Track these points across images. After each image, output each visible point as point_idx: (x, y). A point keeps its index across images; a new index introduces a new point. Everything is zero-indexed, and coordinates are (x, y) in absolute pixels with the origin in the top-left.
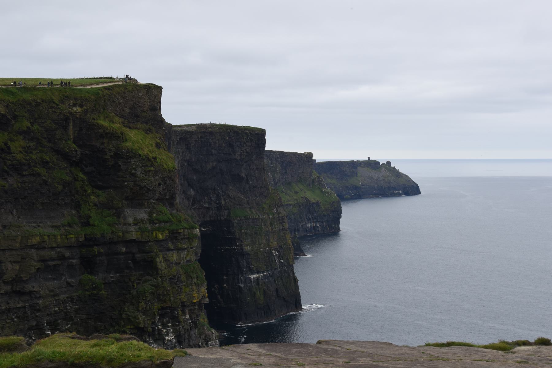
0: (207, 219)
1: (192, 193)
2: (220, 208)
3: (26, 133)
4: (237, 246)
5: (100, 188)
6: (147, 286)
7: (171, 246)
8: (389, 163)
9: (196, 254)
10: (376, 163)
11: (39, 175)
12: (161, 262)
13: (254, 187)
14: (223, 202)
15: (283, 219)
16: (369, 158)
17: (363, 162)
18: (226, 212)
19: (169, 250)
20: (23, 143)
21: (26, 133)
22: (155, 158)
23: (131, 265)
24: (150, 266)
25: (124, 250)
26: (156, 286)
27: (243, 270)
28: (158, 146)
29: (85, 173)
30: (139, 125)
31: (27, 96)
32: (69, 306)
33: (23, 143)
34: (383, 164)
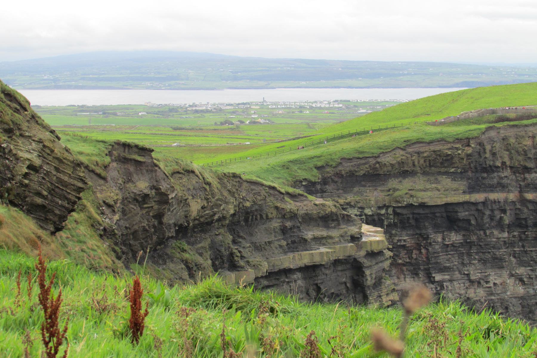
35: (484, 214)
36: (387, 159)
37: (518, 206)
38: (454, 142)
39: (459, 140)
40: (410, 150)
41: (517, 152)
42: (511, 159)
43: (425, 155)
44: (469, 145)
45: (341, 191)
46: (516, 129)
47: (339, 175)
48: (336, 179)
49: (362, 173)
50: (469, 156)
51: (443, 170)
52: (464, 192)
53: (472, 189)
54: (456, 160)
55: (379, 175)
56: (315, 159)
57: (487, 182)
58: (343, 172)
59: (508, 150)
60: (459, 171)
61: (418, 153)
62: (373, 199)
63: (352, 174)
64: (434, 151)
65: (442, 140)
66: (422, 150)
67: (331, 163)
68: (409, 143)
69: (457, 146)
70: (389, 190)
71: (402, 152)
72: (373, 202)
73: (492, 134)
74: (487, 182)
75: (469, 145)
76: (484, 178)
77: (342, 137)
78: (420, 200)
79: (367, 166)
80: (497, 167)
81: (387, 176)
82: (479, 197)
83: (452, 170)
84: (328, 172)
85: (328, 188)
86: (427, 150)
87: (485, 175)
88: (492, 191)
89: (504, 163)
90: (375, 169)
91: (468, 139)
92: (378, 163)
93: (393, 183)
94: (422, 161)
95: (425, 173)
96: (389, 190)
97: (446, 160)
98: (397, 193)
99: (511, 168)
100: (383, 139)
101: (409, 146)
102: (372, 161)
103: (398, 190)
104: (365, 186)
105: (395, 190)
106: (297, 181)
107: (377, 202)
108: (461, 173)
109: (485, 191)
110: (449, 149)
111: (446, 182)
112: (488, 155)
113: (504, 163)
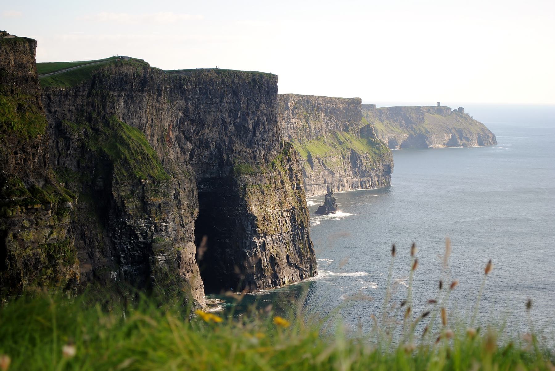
0: (208, 176)
1: (189, 146)
2: (221, 164)
4: (241, 206)
8: (461, 109)
9: (192, 215)
10: (447, 109)
12: (9, 241)
13: (263, 140)
14: (225, 157)
15: (296, 176)
16: (438, 103)
17: (433, 108)
18: (229, 168)
27: (248, 234)
34: (455, 110)
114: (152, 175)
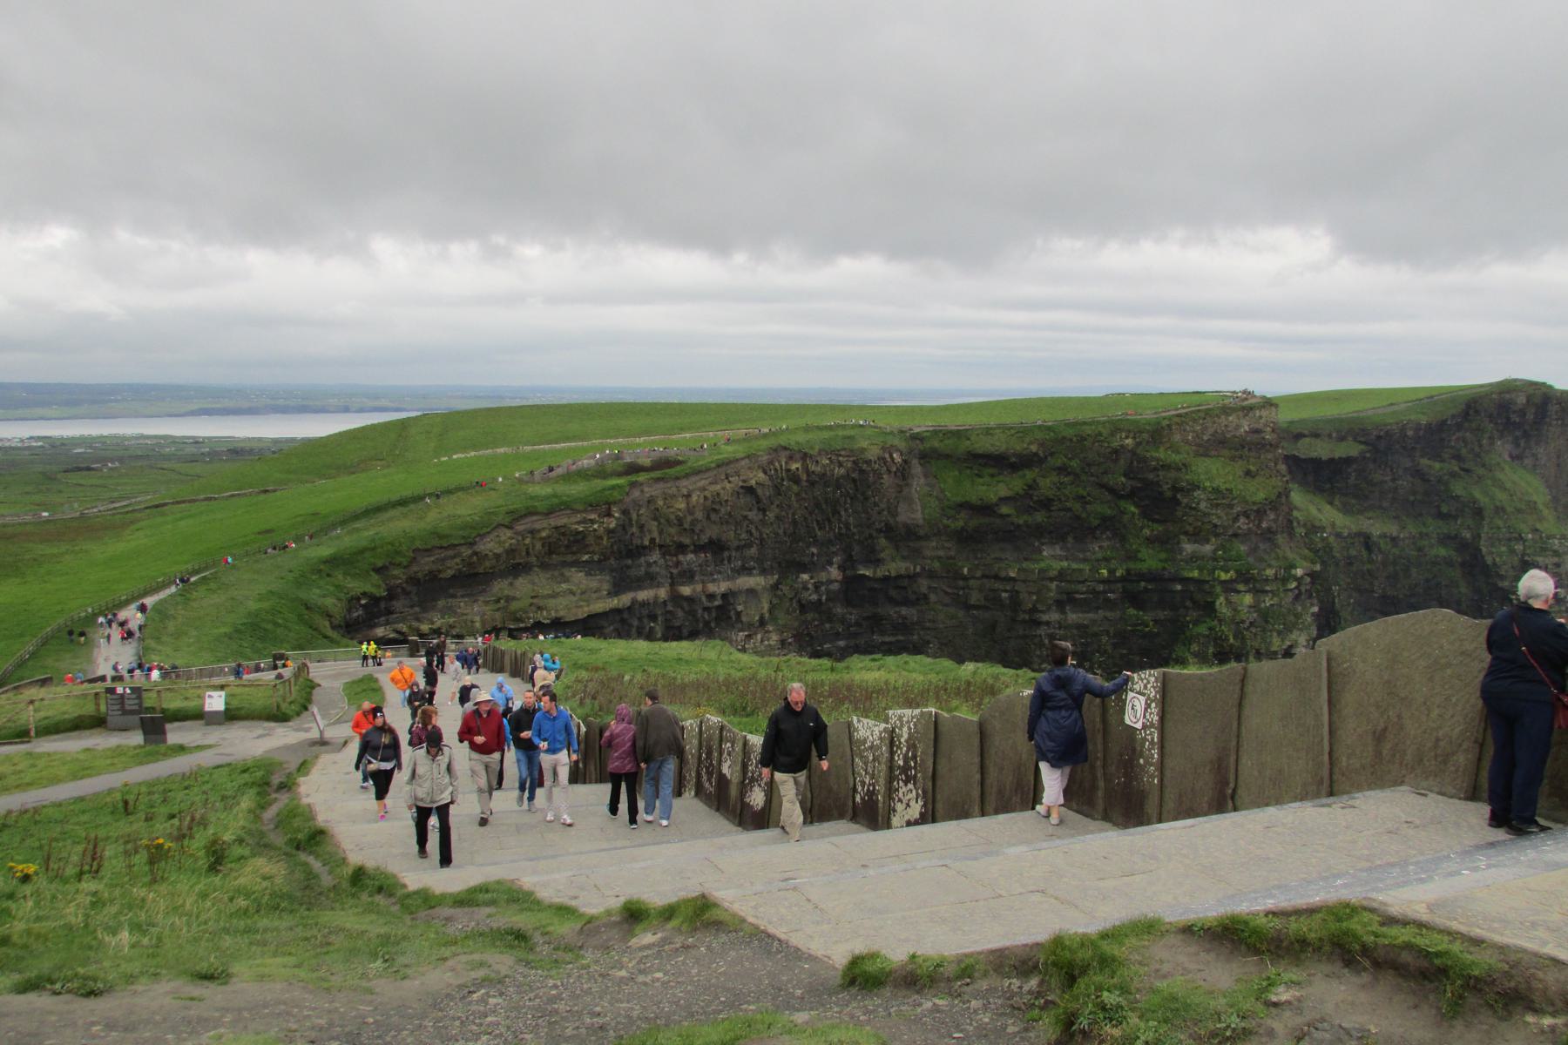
3: (1062, 470)
5: (1154, 521)
6: (1202, 629)
7: (1241, 587)
11: (1070, 510)
19: (1239, 592)
20: (1055, 479)
21: (1062, 470)
22: (1230, 490)
23: (1188, 603)
24: (1209, 609)
25: (1179, 587)
26: (1210, 629)
28: (1248, 473)
29: (1137, 506)
30: (1226, 452)
31: (1069, 433)
32: (1105, 639)
33: (1055, 479)
35: (631, 626)
36: (489, 546)
37: (670, 608)
38: (585, 511)
39: (592, 506)
40: (520, 528)
41: (668, 521)
42: (661, 533)
43: (544, 534)
44: (609, 515)
45: (417, 609)
46: (661, 485)
47: (413, 580)
48: (409, 588)
49: (450, 573)
50: (610, 532)
51: (569, 558)
52: (610, 594)
53: (616, 590)
54: (590, 540)
55: (477, 574)
56: (367, 555)
57: (633, 572)
58: (420, 575)
59: (655, 519)
60: (596, 558)
61: (532, 532)
62: (477, 618)
63: (433, 576)
64: (556, 528)
65: (565, 506)
66: (537, 526)
67: (399, 559)
68: (516, 516)
69: (593, 516)
70: (498, 601)
71: (509, 533)
72: (478, 625)
73: (636, 494)
74: (633, 572)
75: (609, 515)
76: (628, 567)
77: (379, 509)
78: (553, 614)
79: (458, 560)
80: (644, 548)
81: (489, 577)
82: (625, 600)
83: (586, 557)
84: (396, 578)
85: (397, 605)
86: (544, 526)
87: (629, 562)
88: (640, 588)
89: (652, 540)
90: (470, 564)
91: (609, 504)
92: (476, 553)
93: (500, 587)
94: (538, 546)
95: (544, 566)
96: (498, 601)
97: (577, 541)
98: (514, 606)
99: (661, 546)
100: (467, 508)
101: (517, 520)
102: (466, 552)
103: (514, 598)
104: (453, 596)
105: (509, 599)
106: (352, 598)
107: (483, 622)
108: (600, 561)
109: (630, 589)
110: (579, 523)
111: (578, 577)
112: (634, 529)
113: (652, 540)
114: (1538, 526)
